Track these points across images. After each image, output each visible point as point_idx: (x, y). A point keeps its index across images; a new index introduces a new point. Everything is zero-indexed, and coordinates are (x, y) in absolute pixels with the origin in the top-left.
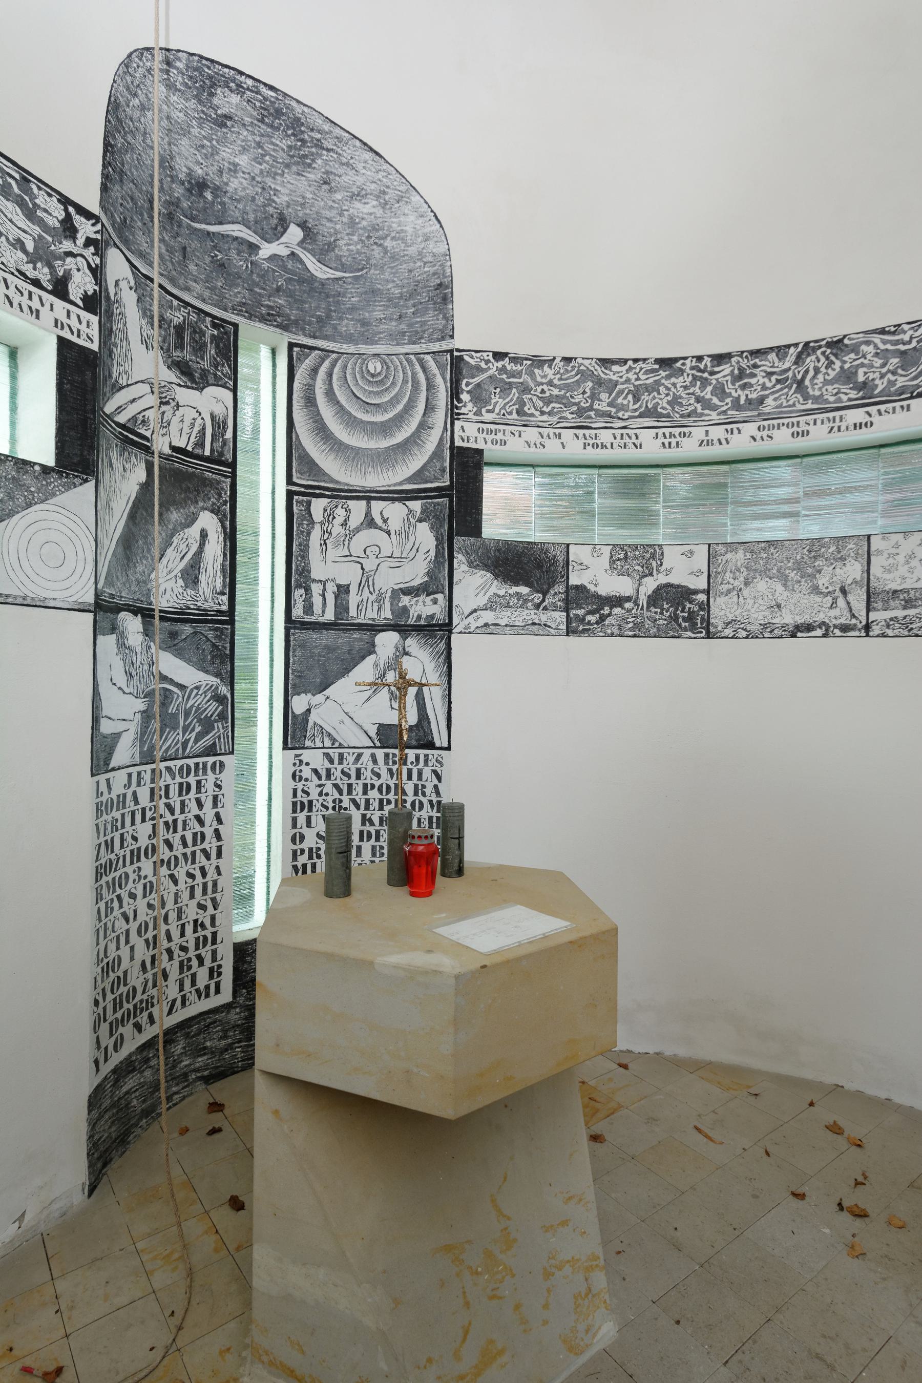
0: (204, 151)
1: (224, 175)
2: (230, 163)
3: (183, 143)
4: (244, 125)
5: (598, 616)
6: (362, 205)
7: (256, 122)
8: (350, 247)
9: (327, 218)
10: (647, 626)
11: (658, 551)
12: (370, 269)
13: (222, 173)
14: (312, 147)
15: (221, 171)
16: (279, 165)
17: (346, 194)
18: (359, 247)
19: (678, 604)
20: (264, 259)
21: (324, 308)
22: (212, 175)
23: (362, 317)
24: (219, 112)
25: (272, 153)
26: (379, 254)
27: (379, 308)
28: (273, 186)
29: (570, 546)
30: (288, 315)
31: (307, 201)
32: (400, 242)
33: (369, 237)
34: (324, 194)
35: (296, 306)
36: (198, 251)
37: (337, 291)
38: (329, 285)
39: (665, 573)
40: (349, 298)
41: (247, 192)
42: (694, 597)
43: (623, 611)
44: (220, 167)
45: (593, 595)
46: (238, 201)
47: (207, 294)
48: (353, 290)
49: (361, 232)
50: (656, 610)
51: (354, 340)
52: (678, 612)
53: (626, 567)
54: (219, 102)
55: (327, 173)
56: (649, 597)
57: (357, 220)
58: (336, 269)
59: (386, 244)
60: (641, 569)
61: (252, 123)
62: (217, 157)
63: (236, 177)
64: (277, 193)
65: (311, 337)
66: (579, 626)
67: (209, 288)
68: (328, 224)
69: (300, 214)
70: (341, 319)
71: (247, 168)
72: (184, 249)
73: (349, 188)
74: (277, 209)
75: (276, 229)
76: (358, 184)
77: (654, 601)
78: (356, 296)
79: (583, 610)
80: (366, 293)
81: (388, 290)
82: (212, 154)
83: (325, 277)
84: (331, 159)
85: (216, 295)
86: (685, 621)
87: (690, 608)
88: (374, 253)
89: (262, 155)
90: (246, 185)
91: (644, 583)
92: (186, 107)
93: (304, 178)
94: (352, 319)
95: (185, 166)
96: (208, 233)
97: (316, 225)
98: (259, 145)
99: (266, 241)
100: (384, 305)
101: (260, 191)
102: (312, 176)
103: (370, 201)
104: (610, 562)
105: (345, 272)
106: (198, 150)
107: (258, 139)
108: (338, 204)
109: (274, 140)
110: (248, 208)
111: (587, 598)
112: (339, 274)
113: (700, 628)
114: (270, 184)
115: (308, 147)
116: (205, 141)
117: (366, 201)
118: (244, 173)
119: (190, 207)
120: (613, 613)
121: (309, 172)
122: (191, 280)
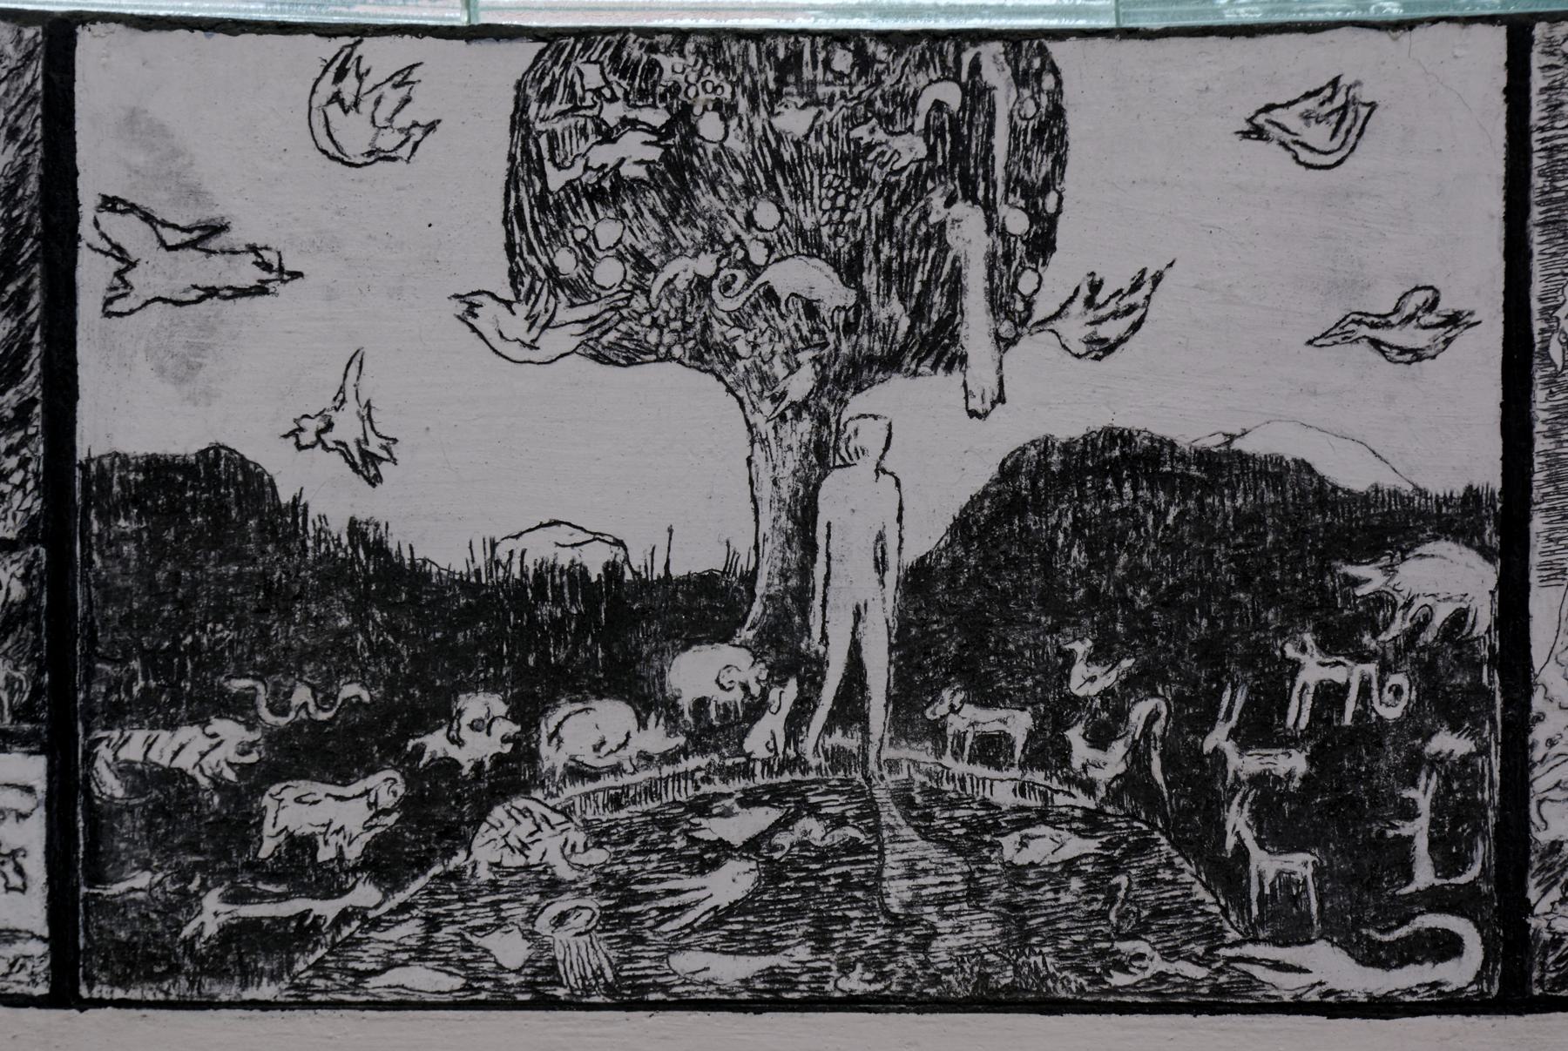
5: (386, 786)
10: (897, 893)
11: (1004, 96)
19: (1212, 652)
29: (88, 44)
39: (1075, 328)
42: (1372, 578)
43: (656, 739)
45: (334, 573)
50: (989, 720)
52: (1218, 738)
53: (683, 269)
56: (918, 579)
60: (831, 292)
66: (189, 902)
77: (975, 627)
79: (230, 731)
86: (1278, 837)
87: (1330, 695)
91: (869, 437)
104: (512, 217)
111: (278, 599)
113: (1436, 900)
120: (552, 758)
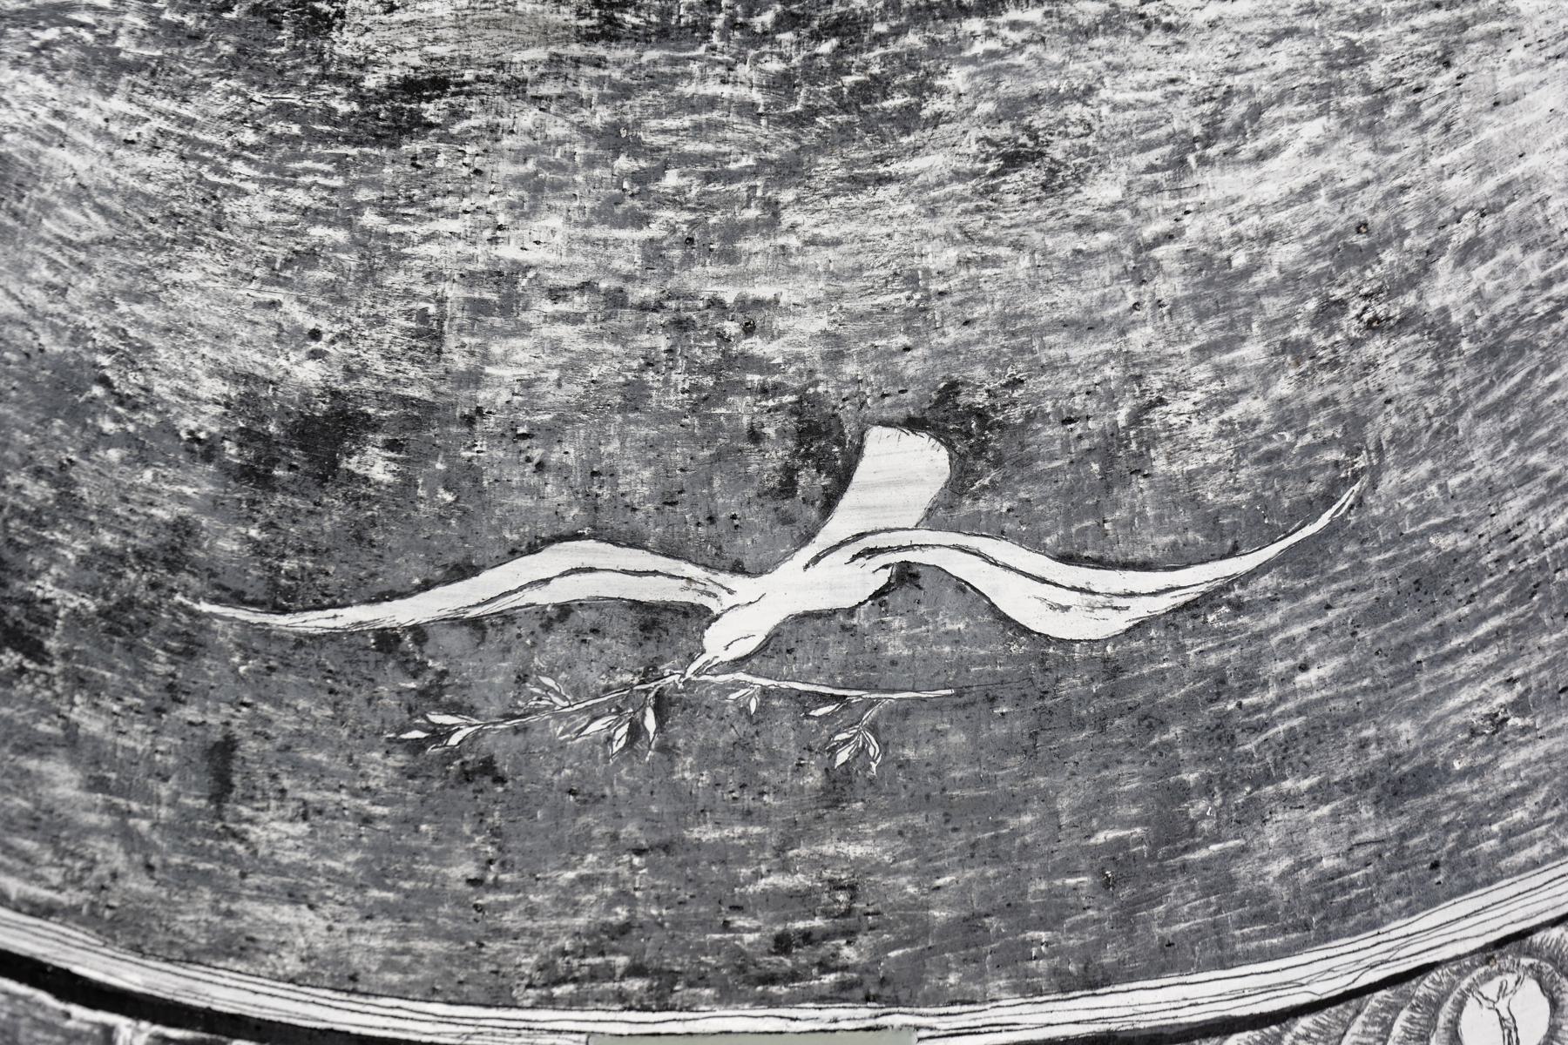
0: (321, 274)
1: (451, 342)
2: (470, 279)
3: (191, 276)
4: (515, 87)
6: (1248, 174)
7: (576, 50)
8: (1234, 412)
9: (1065, 324)
12: (1376, 473)
13: (438, 337)
14: (898, 32)
15: (429, 334)
16: (740, 188)
17: (1140, 161)
18: (1283, 387)
20: (738, 663)
21: (1135, 798)
22: (381, 367)
23: (1375, 754)
24: (370, 82)
25: (691, 147)
26: (1408, 369)
27: (1470, 661)
28: (729, 295)
30: (912, 915)
31: (936, 286)
32: (1513, 251)
33: (1330, 311)
34: (1021, 217)
35: (959, 839)
36: (315, 742)
37: (1202, 674)
38: (1151, 657)
40: (1284, 679)
41: (595, 372)
44: (423, 316)
46: (553, 433)
47: (376, 939)
48: (1299, 630)
49: (1273, 306)
51: (1346, 911)
54: (367, 40)
55: (1012, 109)
57: (1240, 260)
58: (1179, 559)
59: (1434, 303)
61: (555, 60)
62: (395, 280)
63: (523, 330)
64: (758, 317)
65: (1066, 985)
67: (387, 909)
68: (1078, 352)
69: (911, 367)
70: (1251, 815)
71: (571, 269)
72: (224, 751)
73: (1152, 125)
74: (778, 389)
75: (787, 487)
76: (1196, 81)
78: (1322, 654)
80: (1376, 613)
81: (1507, 534)
82: (369, 274)
83: (1118, 623)
84: (1015, 37)
85: (434, 933)
88: (1381, 375)
89: (638, 178)
90: (581, 346)
92: (190, 122)
93: (894, 189)
94: (1320, 794)
95: (218, 372)
96: (387, 640)
97: (1015, 383)
98: (614, 140)
99: (738, 569)
100: (1499, 633)
101: (662, 342)
102: (933, 163)
103: (1284, 131)
105: (1234, 552)
106: (285, 283)
107: (601, 116)
108: (1107, 227)
109: (687, 89)
110: (614, 446)
112: (1198, 577)
114: (709, 290)
115: (879, 39)
116: (318, 232)
117: (1262, 143)
118: (556, 294)
119: (259, 549)
121: (915, 151)
122: (262, 895)
